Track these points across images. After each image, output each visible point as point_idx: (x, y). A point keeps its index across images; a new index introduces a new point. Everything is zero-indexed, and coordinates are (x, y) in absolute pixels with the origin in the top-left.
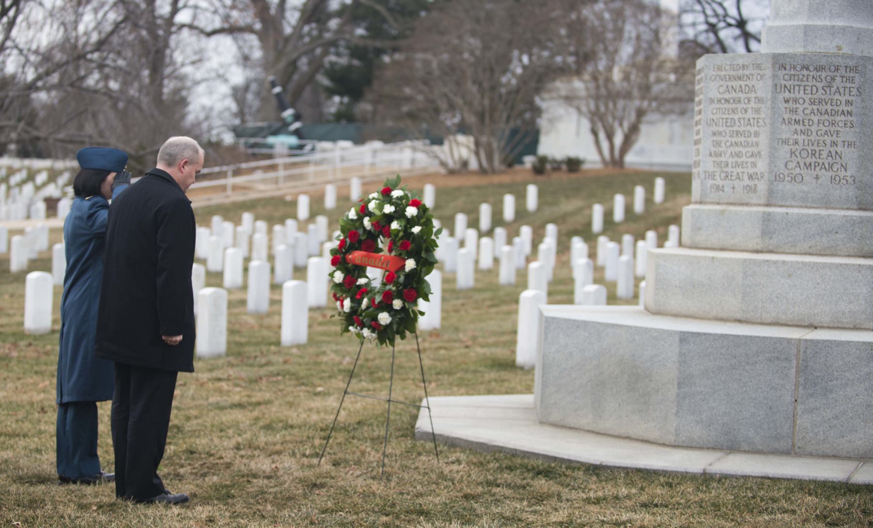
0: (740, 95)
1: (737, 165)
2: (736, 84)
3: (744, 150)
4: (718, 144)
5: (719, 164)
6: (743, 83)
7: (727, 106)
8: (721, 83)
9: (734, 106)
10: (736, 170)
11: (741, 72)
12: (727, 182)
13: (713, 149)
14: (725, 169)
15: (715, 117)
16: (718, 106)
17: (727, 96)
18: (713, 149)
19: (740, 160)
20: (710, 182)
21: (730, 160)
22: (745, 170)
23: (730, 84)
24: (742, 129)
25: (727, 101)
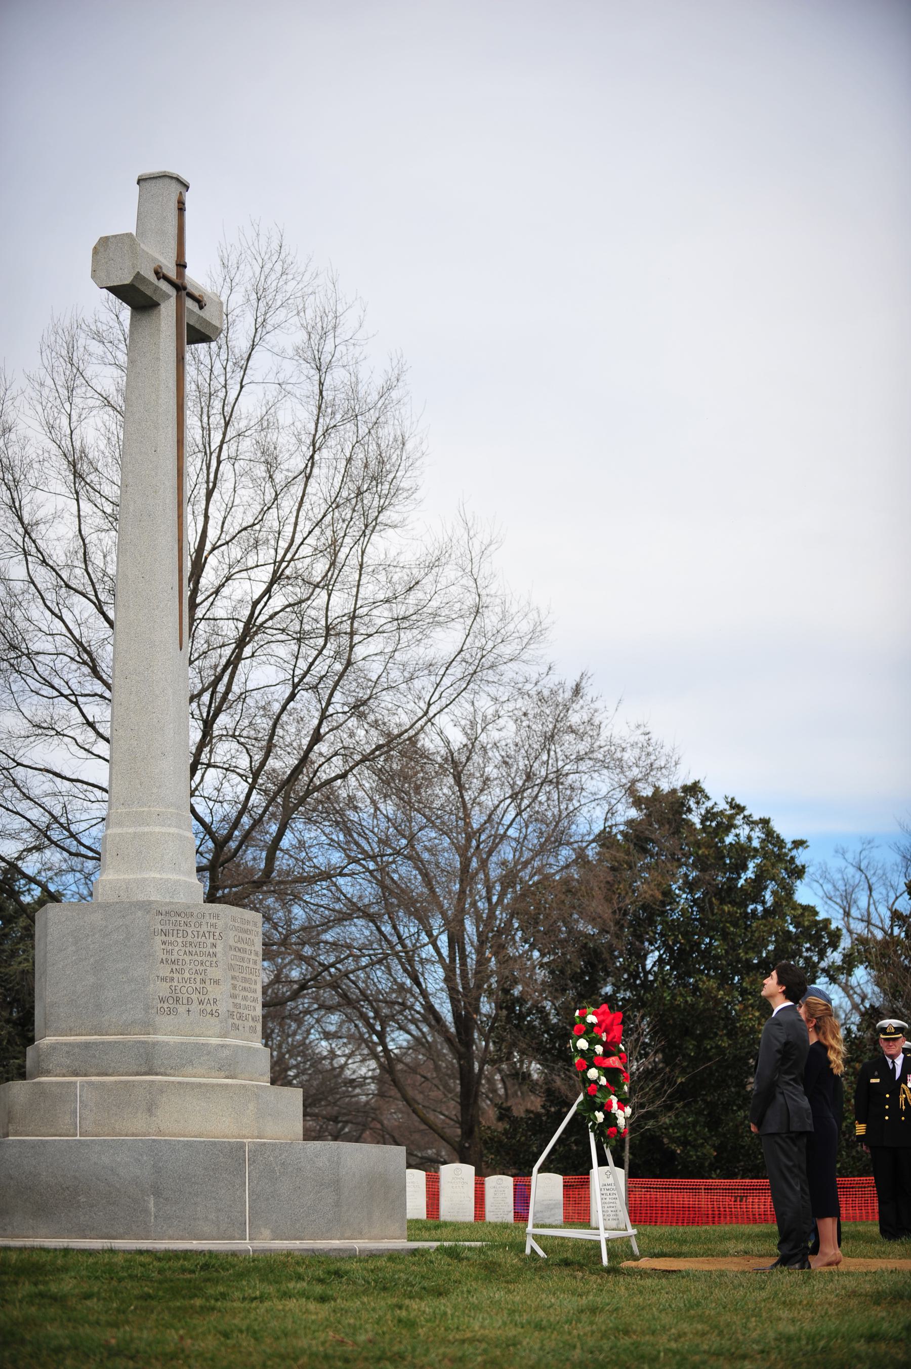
0: (246, 946)
1: (246, 1007)
2: (244, 936)
3: (250, 995)
4: (234, 987)
5: (236, 1005)
6: (248, 937)
7: (238, 954)
8: (236, 933)
9: (242, 955)
10: (246, 1012)
11: (246, 927)
12: (240, 1022)
13: (232, 991)
14: (239, 1010)
15: (233, 962)
16: (235, 953)
17: (239, 945)
18: (232, 991)
19: (247, 1003)
20: (230, 1021)
21: (243, 1003)
22: (250, 1012)
23: (240, 935)
24: (247, 976)
25: (240, 950)
